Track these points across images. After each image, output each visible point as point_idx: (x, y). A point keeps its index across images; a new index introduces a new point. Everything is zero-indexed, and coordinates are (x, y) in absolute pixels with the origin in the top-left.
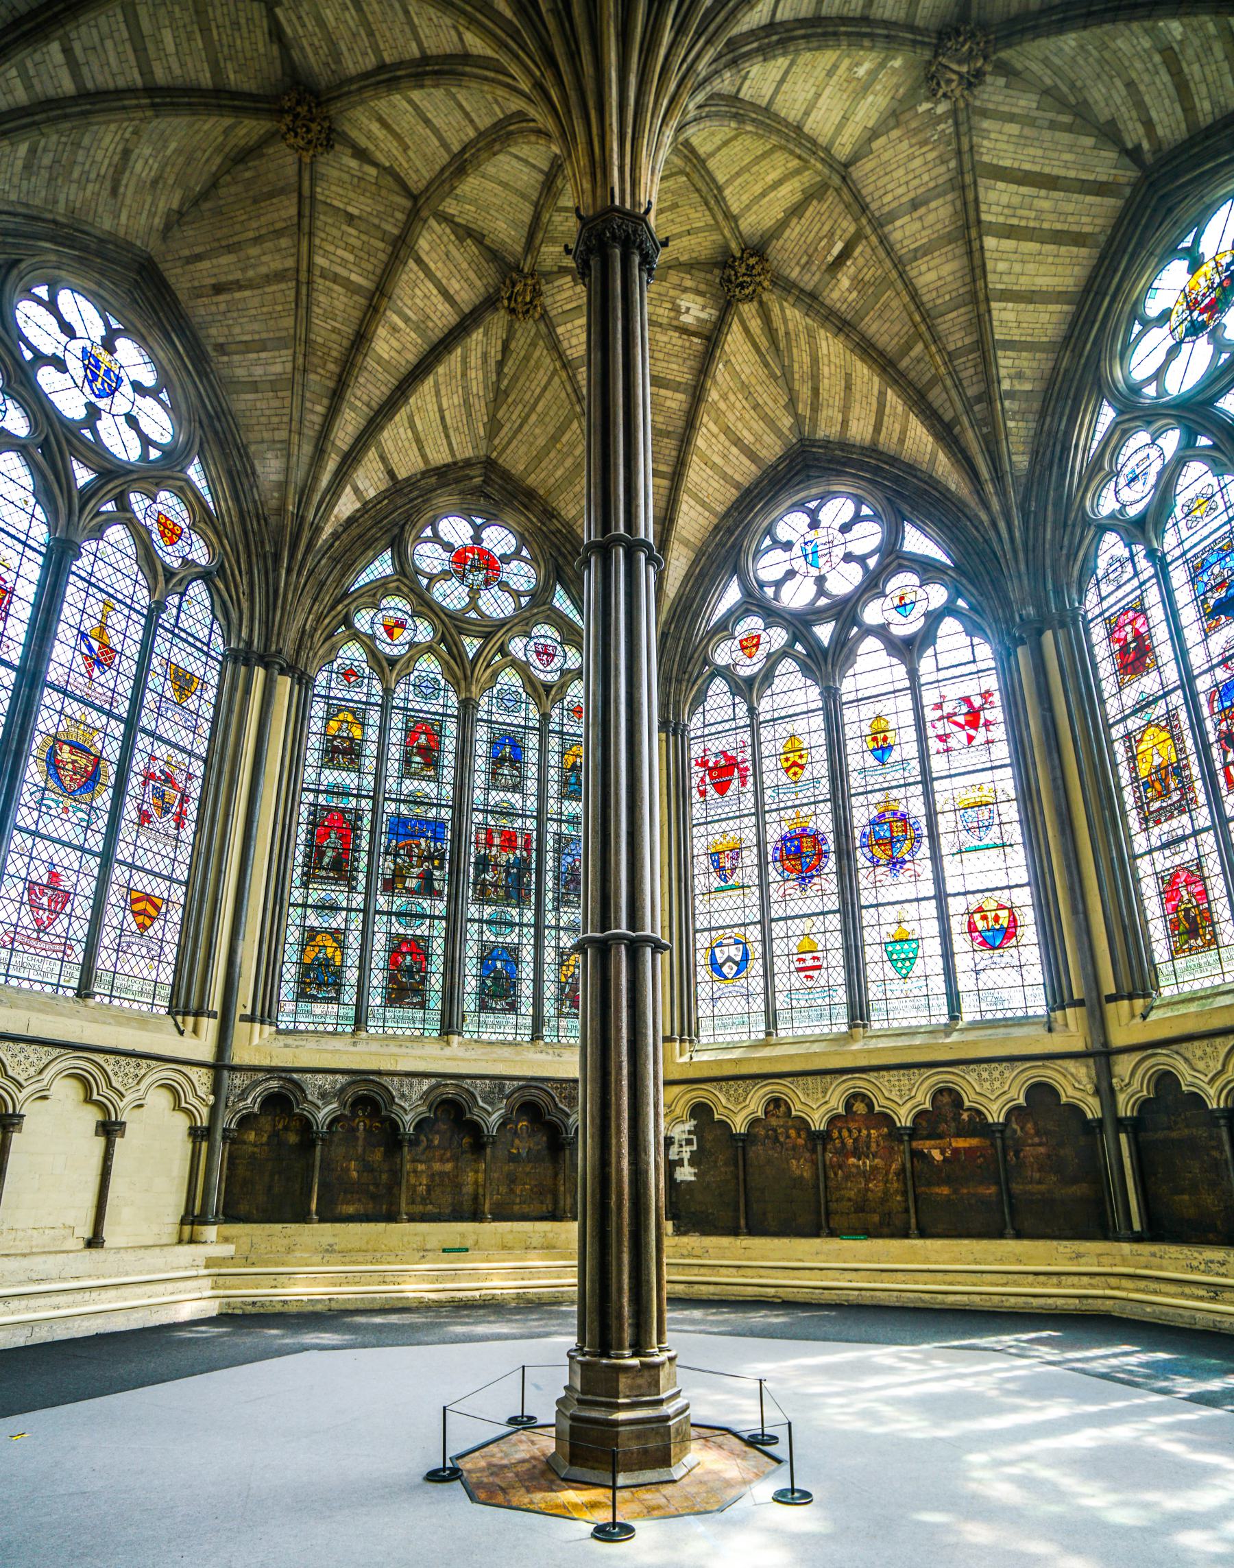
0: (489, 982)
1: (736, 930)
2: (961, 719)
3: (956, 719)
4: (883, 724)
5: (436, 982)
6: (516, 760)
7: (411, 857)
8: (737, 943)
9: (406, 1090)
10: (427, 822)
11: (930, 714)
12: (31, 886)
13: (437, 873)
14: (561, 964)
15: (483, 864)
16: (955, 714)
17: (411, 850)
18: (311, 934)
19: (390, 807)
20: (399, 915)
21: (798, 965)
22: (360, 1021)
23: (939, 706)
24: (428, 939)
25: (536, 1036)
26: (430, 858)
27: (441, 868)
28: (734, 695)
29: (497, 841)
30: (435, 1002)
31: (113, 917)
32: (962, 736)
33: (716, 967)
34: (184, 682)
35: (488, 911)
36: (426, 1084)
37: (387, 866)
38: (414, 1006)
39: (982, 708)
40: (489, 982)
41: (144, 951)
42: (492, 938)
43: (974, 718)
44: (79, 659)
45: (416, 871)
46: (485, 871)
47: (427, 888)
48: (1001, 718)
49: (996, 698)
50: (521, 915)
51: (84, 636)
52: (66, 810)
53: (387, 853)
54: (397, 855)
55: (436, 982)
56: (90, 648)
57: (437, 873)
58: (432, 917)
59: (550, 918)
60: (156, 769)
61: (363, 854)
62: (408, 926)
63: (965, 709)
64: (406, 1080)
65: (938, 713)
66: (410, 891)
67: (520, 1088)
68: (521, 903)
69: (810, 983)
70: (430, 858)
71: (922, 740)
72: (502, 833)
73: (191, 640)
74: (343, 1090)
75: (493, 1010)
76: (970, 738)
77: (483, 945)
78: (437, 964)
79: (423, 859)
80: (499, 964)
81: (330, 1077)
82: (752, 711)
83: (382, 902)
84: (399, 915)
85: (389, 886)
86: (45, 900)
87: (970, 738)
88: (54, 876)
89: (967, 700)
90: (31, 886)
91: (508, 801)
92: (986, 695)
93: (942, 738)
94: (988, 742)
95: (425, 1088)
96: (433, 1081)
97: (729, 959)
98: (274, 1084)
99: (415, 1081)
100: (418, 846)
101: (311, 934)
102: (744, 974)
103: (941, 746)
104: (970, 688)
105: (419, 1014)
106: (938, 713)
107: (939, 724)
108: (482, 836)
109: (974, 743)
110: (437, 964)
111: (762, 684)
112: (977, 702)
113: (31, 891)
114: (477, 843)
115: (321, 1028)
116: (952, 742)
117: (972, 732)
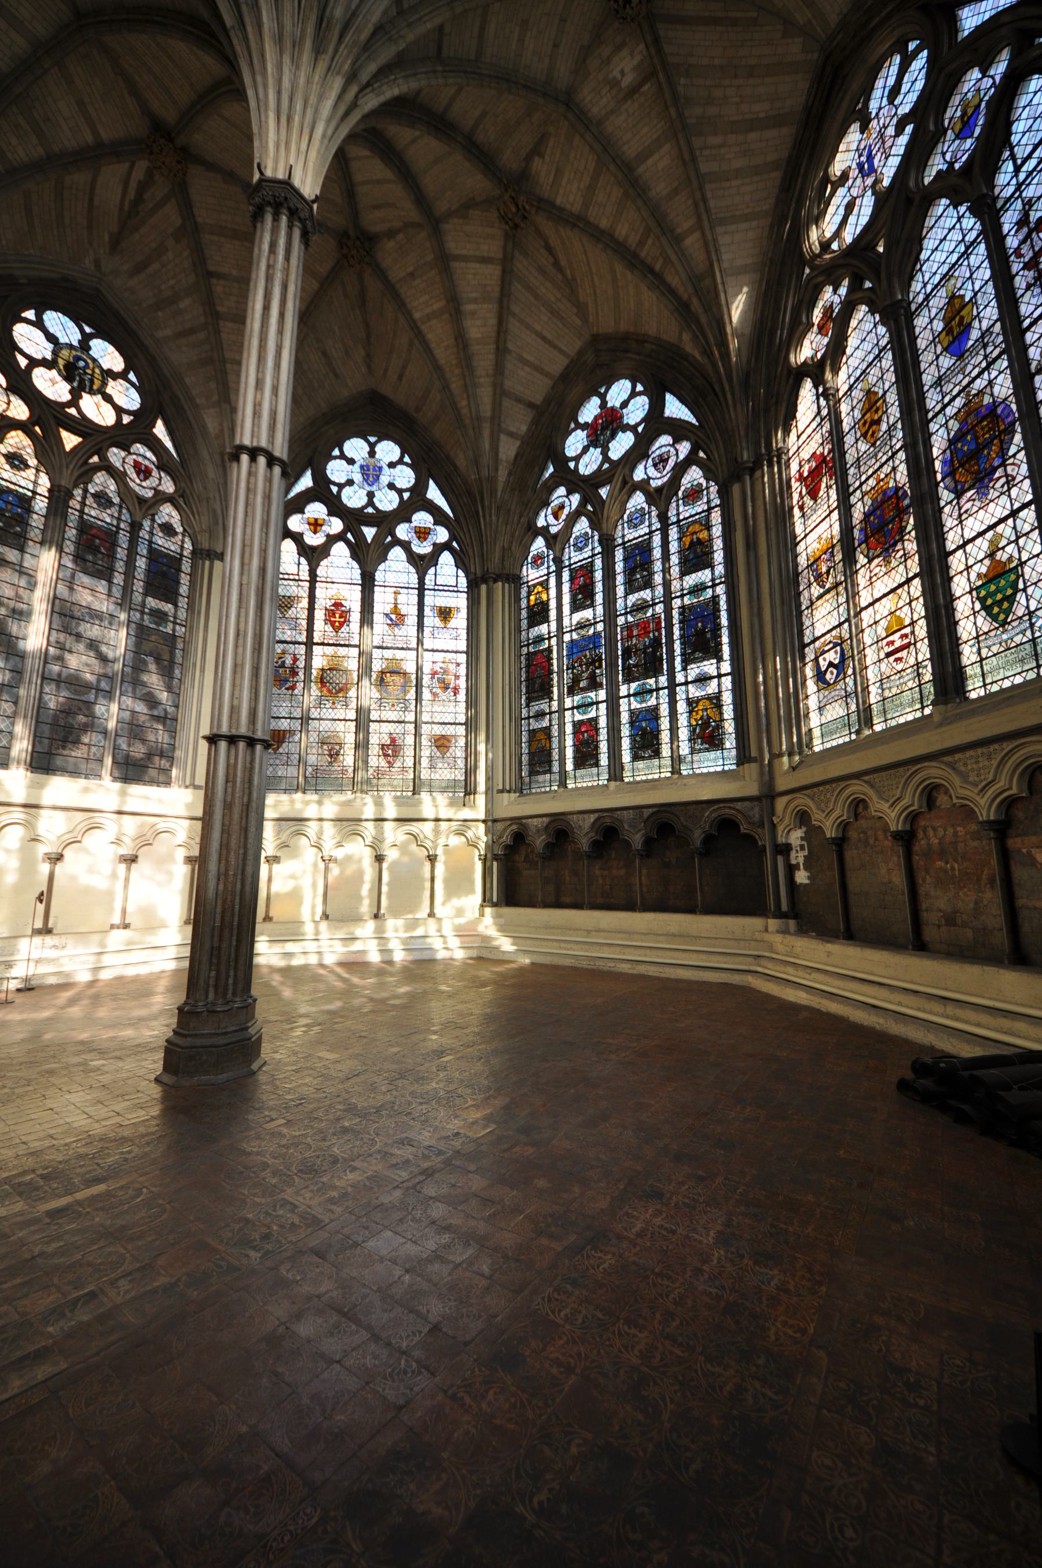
0: (638, 739)
1: (834, 633)
5: (603, 747)
6: (646, 564)
7: (581, 666)
8: (836, 645)
9: (581, 823)
10: (589, 637)
12: (383, 747)
13: (598, 671)
14: (690, 712)
15: (627, 653)
17: (582, 661)
18: (532, 733)
19: (567, 638)
20: (578, 707)
21: (887, 649)
22: (563, 784)
24: (595, 720)
25: (675, 771)
26: (593, 663)
27: (600, 667)
29: (635, 633)
30: (604, 760)
31: (426, 752)
33: (820, 676)
34: (445, 614)
35: (634, 686)
36: (593, 817)
37: (567, 677)
38: (591, 766)
40: (638, 739)
41: (446, 765)
42: (639, 706)
44: (387, 627)
45: (585, 675)
46: (630, 658)
47: (594, 685)
50: (657, 682)
51: (387, 615)
52: (393, 705)
53: (568, 669)
54: (574, 668)
55: (603, 747)
56: (391, 620)
57: (598, 671)
58: (597, 703)
59: (680, 678)
60: (437, 668)
61: (555, 675)
62: (585, 713)
64: (581, 816)
66: (584, 690)
67: (653, 814)
68: (656, 672)
69: (899, 667)
70: (593, 663)
72: (638, 625)
73: (446, 588)
74: (547, 827)
75: (643, 758)
77: (632, 712)
78: (603, 735)
79: (588, 665)
80: (644, 724)
81: (540, 820)
83: (568, 703)
84: (578, 707)
85: (571, 692)
86: (390, 752)
88: (393, 740)
90: (383, 747)
91: (642, 599)
95: (592, 820)
96: (597, 815)
97: (831, 664)
98: (514, 827)
99: (586, 816)
100: (585, 656)
101: (532, 733)
102: (842, 676)
105: (595, 770)
108: (625, 633)
110: (603, 735)
113: (383, 749)
114: (622, 639)
115: (543, 790)
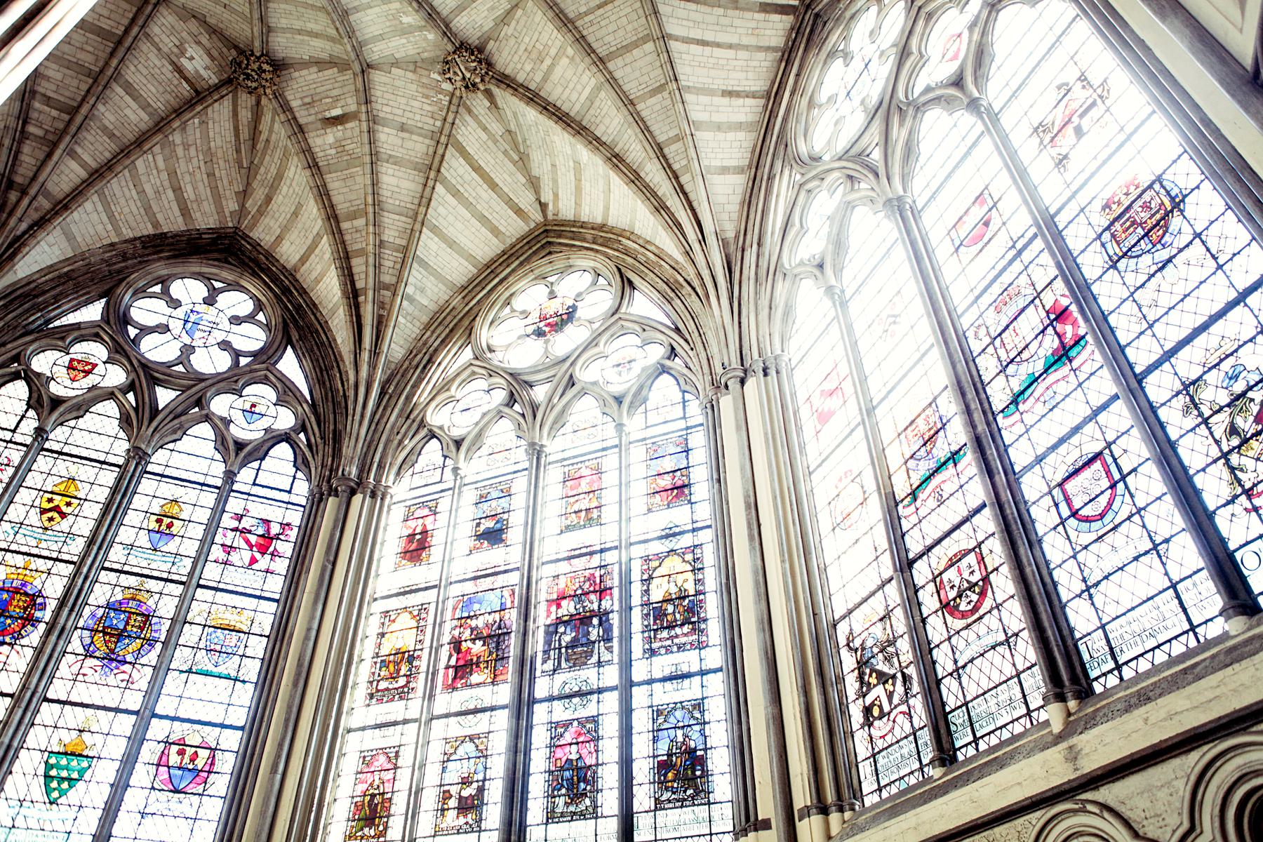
2: (253, 539)
3: (249, 536)
4: (175, 510)
11: (227, 521)
16: (250, 532)
23: (239, 518)
28: (29, 406)
32: (247, 555)
39: (277, 537)
43: (265, 544)
48: (289, 554)
49: (293, 534)
63: (261, 531)
65: (235, 524)
71: (207, 541)
76: (253, 561)
82: (40, 433)
87: (253, 561)
89: (267, 522)
92: (285, 526)
93: (228, 549)
94: (267, 571)
103: (222, 556)
104: (275, 514)
106: (235, 524)
107: (230, 534)
109: (254, 566)
111: (70, 410)
112: (275, 529)
116: (234, 557)
117: (258, 556)
